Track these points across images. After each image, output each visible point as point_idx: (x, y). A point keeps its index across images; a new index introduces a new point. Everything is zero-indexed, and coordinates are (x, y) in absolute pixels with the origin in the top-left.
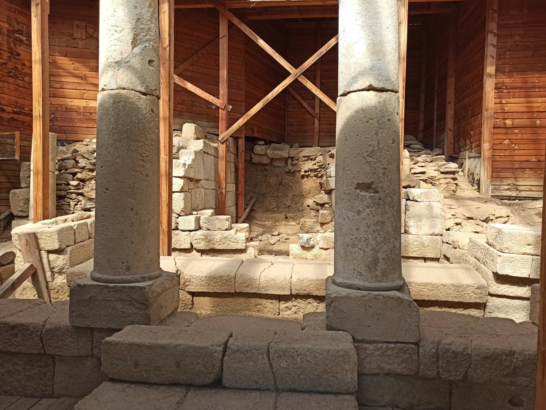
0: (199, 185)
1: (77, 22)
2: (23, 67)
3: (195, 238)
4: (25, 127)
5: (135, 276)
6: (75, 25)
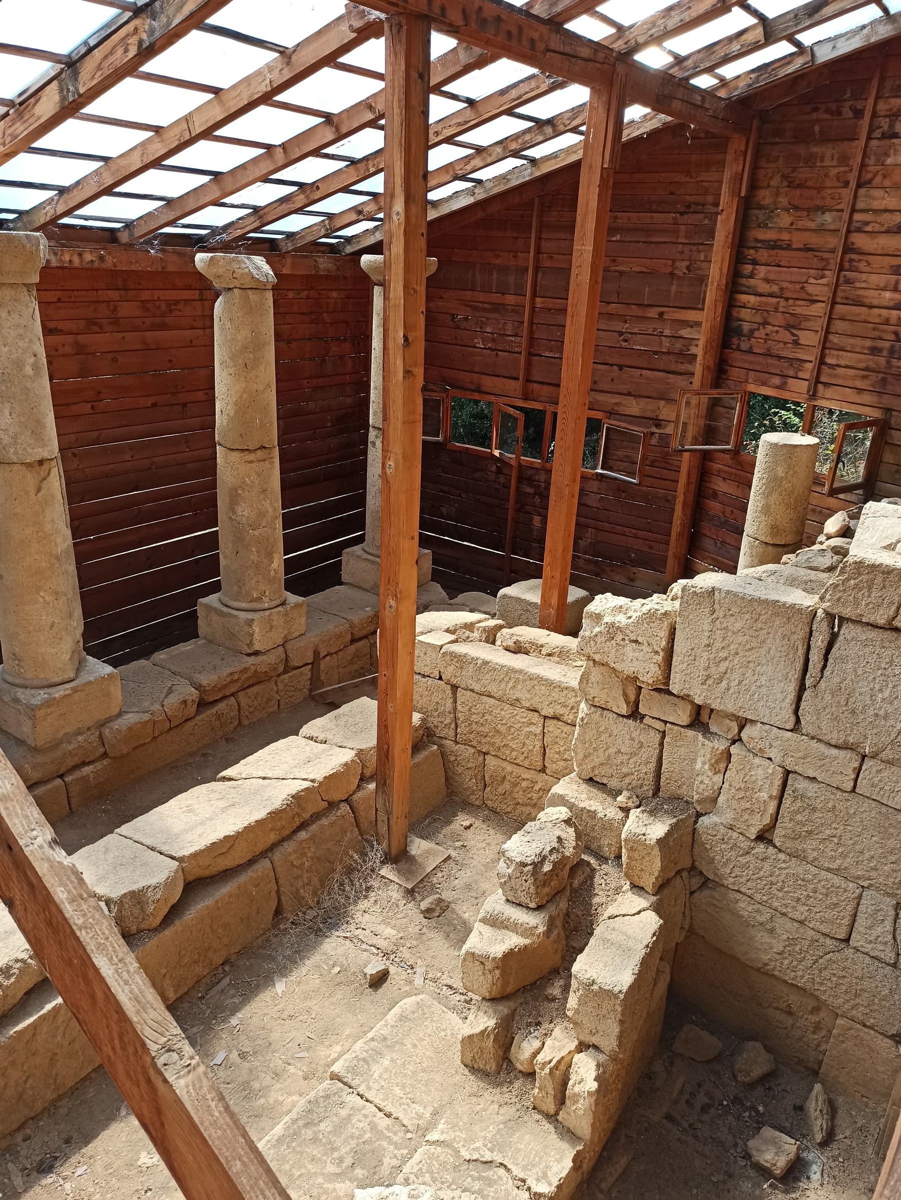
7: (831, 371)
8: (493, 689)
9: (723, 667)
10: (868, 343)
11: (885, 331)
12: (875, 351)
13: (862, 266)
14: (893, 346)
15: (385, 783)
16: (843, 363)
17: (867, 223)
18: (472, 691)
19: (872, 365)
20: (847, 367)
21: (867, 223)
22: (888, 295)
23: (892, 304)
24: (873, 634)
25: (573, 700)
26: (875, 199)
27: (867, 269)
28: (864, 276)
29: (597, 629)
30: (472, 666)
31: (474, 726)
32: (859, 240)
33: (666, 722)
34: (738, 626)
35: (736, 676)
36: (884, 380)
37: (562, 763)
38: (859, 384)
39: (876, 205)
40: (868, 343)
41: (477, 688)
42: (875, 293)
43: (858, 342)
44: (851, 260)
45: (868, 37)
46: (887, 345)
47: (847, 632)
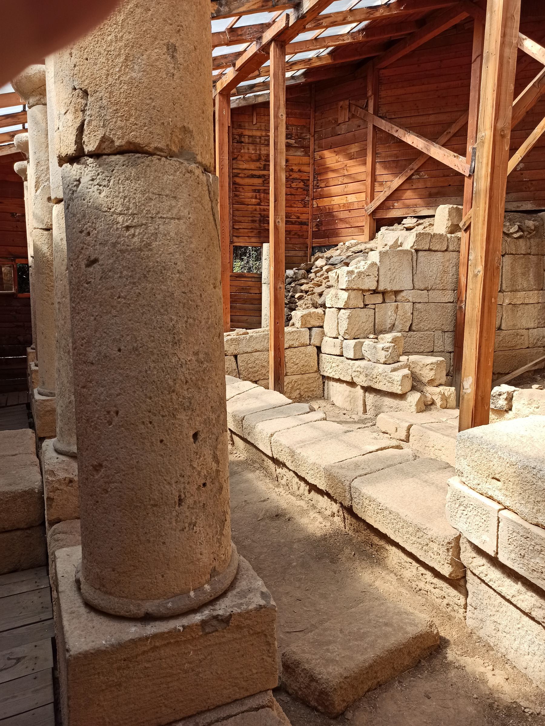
0: (399, 298)
1: (341, 103)
2: (291, 173)
3: (354, 369)
4: (292, 236)
5: (46, 391)
6: (339, 108)
7: (237, 231)
8: (258, 347)
9: (394, 274)
10: (250, 219)
11: (255, 214)
12: (253, 221)
13: (241, 189)
14: (260, 219)
15: (279, 379)
16: (241, 227)
17: (239, 174)
18: (246, 353)
19: (254, 227)
20: (244, 229)
21: (239, 174)
22: (254, 200)
23: (256, 203)
24: (426, 253)
25: (297, 335)
26: (240, 164)
27: (243, 191)
28: (243, 194)
29: (353, 276)
30: (244, 340)
31: (250, 370)
32: (238, 180)
33: (375, 304)
34: (396, 260)
35: (397, 277)
36: (259, 232)
37: (296, 366)
38: (250, 235)
39: (241, 167)
40: (250, 219)
41: (249, 350)
42: (249, 200)
43: (246, 218)
44: (236, 188)
45: (238, 104)
46: (258, 219)
47: (420, 254)
